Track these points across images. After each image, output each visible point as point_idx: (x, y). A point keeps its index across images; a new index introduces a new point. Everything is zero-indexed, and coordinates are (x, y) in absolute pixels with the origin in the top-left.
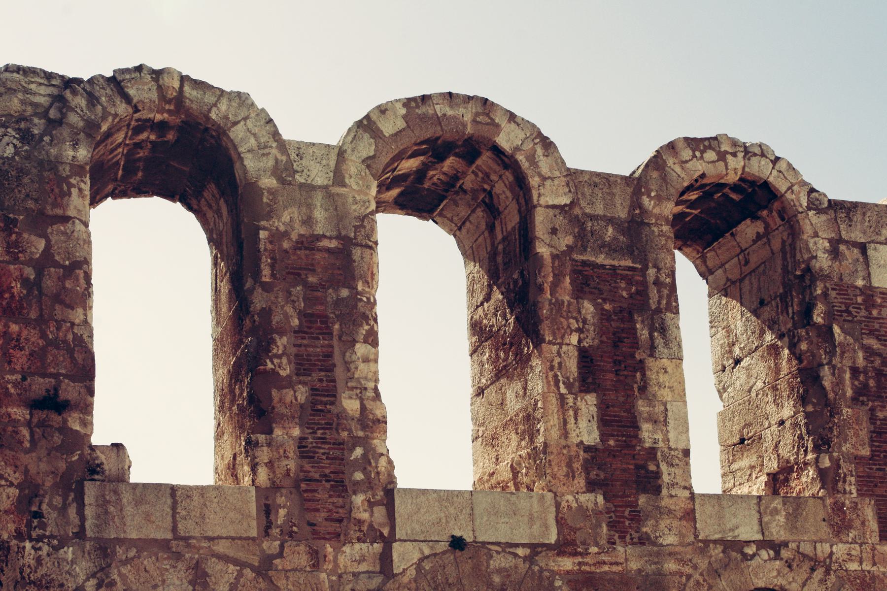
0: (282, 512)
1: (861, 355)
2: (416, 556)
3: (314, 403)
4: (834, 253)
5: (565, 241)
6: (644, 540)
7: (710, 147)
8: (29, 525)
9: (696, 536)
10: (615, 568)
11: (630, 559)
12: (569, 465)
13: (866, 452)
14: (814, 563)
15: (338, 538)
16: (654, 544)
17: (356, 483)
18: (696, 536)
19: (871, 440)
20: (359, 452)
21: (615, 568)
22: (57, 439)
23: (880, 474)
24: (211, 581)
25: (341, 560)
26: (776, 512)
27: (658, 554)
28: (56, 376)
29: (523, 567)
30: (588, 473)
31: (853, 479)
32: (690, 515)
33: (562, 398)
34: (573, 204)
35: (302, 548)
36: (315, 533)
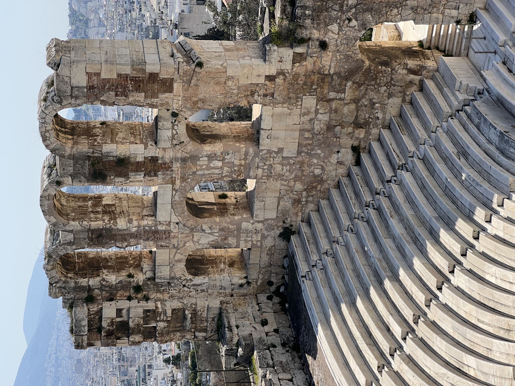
0: (162, 243)
1: (110, 92)
2: (175, 216)
4: (77, 98)
7: (44, 134)
10: (179, 170)
12: (150, 180)
13: (143, 94)
15: (170, 232)
17: (155, 229)
19: (139, 92)
20: (147, 228)
21: (179, 170)
23: (150, 90)
26: (163, 124)
32: (164, 149)
33: (130, 182)
34: (71, 176)
35: (172, 240)
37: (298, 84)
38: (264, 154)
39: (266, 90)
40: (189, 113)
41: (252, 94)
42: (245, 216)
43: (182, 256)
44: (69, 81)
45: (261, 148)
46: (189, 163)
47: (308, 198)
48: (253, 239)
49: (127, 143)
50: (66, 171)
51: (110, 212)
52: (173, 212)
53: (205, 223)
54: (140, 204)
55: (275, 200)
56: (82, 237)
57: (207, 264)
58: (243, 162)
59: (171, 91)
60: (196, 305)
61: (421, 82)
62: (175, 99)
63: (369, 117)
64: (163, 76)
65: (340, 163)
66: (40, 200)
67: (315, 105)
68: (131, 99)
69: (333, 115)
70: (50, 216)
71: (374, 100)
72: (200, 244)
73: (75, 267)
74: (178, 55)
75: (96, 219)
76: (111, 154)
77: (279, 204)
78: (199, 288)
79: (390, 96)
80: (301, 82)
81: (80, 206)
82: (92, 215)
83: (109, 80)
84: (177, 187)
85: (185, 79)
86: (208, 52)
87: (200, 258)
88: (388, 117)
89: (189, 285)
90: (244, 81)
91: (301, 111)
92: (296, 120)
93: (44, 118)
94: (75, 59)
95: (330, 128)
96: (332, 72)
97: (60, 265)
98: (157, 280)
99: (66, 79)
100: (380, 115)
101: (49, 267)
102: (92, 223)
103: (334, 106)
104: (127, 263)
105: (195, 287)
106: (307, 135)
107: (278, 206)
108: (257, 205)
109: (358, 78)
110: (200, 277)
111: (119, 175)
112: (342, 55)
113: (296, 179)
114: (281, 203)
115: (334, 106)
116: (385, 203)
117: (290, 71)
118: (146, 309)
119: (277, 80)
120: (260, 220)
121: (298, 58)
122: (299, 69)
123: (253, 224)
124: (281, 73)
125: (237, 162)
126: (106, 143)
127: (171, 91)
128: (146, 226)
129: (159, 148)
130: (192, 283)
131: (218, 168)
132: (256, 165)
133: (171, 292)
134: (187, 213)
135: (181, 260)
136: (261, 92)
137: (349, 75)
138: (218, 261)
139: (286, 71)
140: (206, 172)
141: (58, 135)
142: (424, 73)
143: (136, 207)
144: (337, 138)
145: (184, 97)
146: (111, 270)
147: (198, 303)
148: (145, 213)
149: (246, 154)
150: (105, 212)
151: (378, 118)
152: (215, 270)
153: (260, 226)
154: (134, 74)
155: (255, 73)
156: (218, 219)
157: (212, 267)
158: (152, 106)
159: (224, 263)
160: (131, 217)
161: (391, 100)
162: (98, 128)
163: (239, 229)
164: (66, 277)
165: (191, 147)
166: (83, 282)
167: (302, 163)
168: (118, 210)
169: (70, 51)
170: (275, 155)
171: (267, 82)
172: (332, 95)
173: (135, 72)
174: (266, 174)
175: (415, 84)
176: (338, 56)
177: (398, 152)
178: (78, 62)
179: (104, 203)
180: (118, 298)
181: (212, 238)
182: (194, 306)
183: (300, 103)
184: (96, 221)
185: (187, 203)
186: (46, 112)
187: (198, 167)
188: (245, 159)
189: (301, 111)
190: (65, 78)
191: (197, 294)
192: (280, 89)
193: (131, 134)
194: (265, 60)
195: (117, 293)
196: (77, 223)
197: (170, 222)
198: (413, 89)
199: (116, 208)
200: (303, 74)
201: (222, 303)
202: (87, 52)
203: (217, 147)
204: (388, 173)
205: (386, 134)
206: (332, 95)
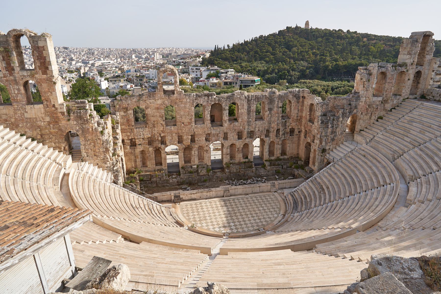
4: (33, 42)
32: (18, 73)
41: (46, 101)
45: (26, 106)
46: (14, 82)
55: (5, 113)
59: (42, 74)
61: (62, 151)
62: (40, 76)
64: (48, 72)
68: (37, 61)
79: (55, 143)
84: (3, 78)
90: (51, 98)
92: (40, 115)
95: (39, 127)
99: (40, 39)
109: (60, 133)
113: (16, 119)
116: (19, 149)
121: (63, 113)
122: (60, 115)
124: (56, 109)
125: (18, 98)
127: (42, 74)
136: (48, 104)
137: (61, 130)
154: (47, 62)
155: (55, 101)
161: (53, 144)
165: (22, 82)
167: (23, 120)
172: (52, 126)
188: (20, 101)
206: (52, 126)
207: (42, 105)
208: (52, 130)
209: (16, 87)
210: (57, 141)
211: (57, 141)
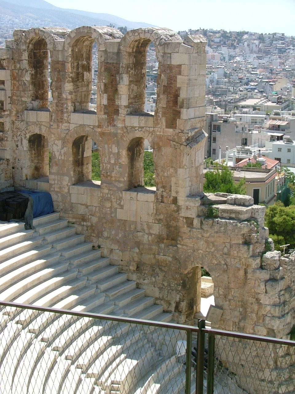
0: (54, 117)
2: (74, 127)
3: (58, 96)
4: (163, 56)
5: (103, 59)
6: (114, 126)
7: (137, 32)
8: (17, 119)
9: (125, 125)
10: (108, 131)
11: (111, 129)
13: (165, 106)
14: (149, 132)
16: (116, 126)
18: (125, 125)
19: (167, 103)
20: (65, 105)
21: (108, 131)
22: (21, 103)
23: (167, 111)
24: (42, 130)
25: (62, 127)
26: (142, 120)
27: (117, 129)
28: (20, 91)
29: (91, 130)
30: (104, 111)
31: (161, 113)
32: (124, 120)
33: (100, 94)
35: (56, 124)
36: (58, 121)
37: (170, 221)
38: (119, 195)
39: (166, 197)
40: (151, 140)
41: (163, 187)
42: (73, 179)
43: (44, 131)
44: (175, 51)
47: (86, 226)
48: (56, 185)
49: (129, 92)
50: (109, 46)
51: (78, 77)
52: (77, 125)
53: (69, 149)
54: (83, 100)
56: (60, 56)
57: (37, 150)
58: (114, 179)
59: (167, 127)
60: (7, 140)
63: (145, 274)
64: (178, 122)
65: (111, 251)
66: (87, 27)
67: (154, 233)
69: (147, 247)
70: (75, 33)
71: (157, 277)
72: (53, 145)
73: (36, 50)
74: (193, 133)
75: (73, 68)
76: (121, 81)
77: (82, 205)
78: (19, 143)
79: (161, 289)
80: (171, 223)
81: (82, 55)
82: (76, 64)
83: (175, 81)
85: (176, 137)
86: (195, 155)
87: (42, 143)
88: (144, 287)
89: (22, 135)
90: (173, 180)
91: (150, 223)
92: (145, 218)
93: (148, 32)
94: (192, 57)
95: (138, 244)
96: (179, 246)
97: (38, 39)
98: (25, 112)
99: (177, 50)
100: (146, 281)
101: (37, 31)
102: (70, 65)
103: (154, 247)
104: (39, 89)
105: (20, 140)
106: (133, 227)
107: (80, 204)
108: (81, 189)
110: (28, 144)
111: (105, 85)
112: (191, 254)
114: (83, 207)
115: (154, 247)
117: (180, 215)
118: (4, 102)
119: (173, 205)
120: (70, 190)
121: (189, 222)
123: (67, 185)
124: (178, 209)
126: (130, 77)
127: (167, 127)
128: (67, 105)
129: (125, 117)
130: (23, 138)
131: (109, 160)
132: (111, 189)
133: (17, 122)
134: (76, 136)
135: (41, 130)
136: (164, 194)
138: (40, 158)
139: (180, 212)
140: (107, 151)
141: (136, 41)
142: (177, 314)
143: (82, 97)
144: (130, 249)
145: (163, 137)
146: (34, 77)
147: (8, 142)
148: (77, 104)
149: (119, 182)
150: (78, 74)
151: (144, 280)
152: (33, 156)
153: (66, 190)
155: (179, 189)
156: (71, 159)
157: (35, 154)
158: (156, 112)
159: (38, 163)
160: (74, 94)
161: (157, 289)
162: (141, 70)
163: (63, 175)
164: (29, 43)
166: (25, 56)
168: (80, 84)
169: (197, 53)
170: (118, 203)
171: (172, 198)
173: (181, 100)
174: (104, 196)
175: (168, 307)
176: (190, 251)
177: (118, 294)
178: (190, 59)
179: (85, 73)
180: (13, 82)
181: (57, 154)
182: (6, 139)
183: (157, 222)
184: (71, 67)
185: (83, 137)
186: (153, 34)
187: (110, 146)
188: (116, 181)
189: (150, 223)
190: (178, 48)
191: (15, 142)
192: (167, 208)
193: (136, 96)
194: (188, 197)
195: (17, 81)
196: (70, 53)
197: (70, 123)
198: (165, 306)
199: (81, 82)
200: (178, 225)
201: (8, 160)
202: (196, 65)
203: (124, 159)
204: (103, 286)
205: (133, 285)
207: (152, 195)
208: (161, 257)
209: (115, 150)
210: (166, 284)
211: (166, 284)
